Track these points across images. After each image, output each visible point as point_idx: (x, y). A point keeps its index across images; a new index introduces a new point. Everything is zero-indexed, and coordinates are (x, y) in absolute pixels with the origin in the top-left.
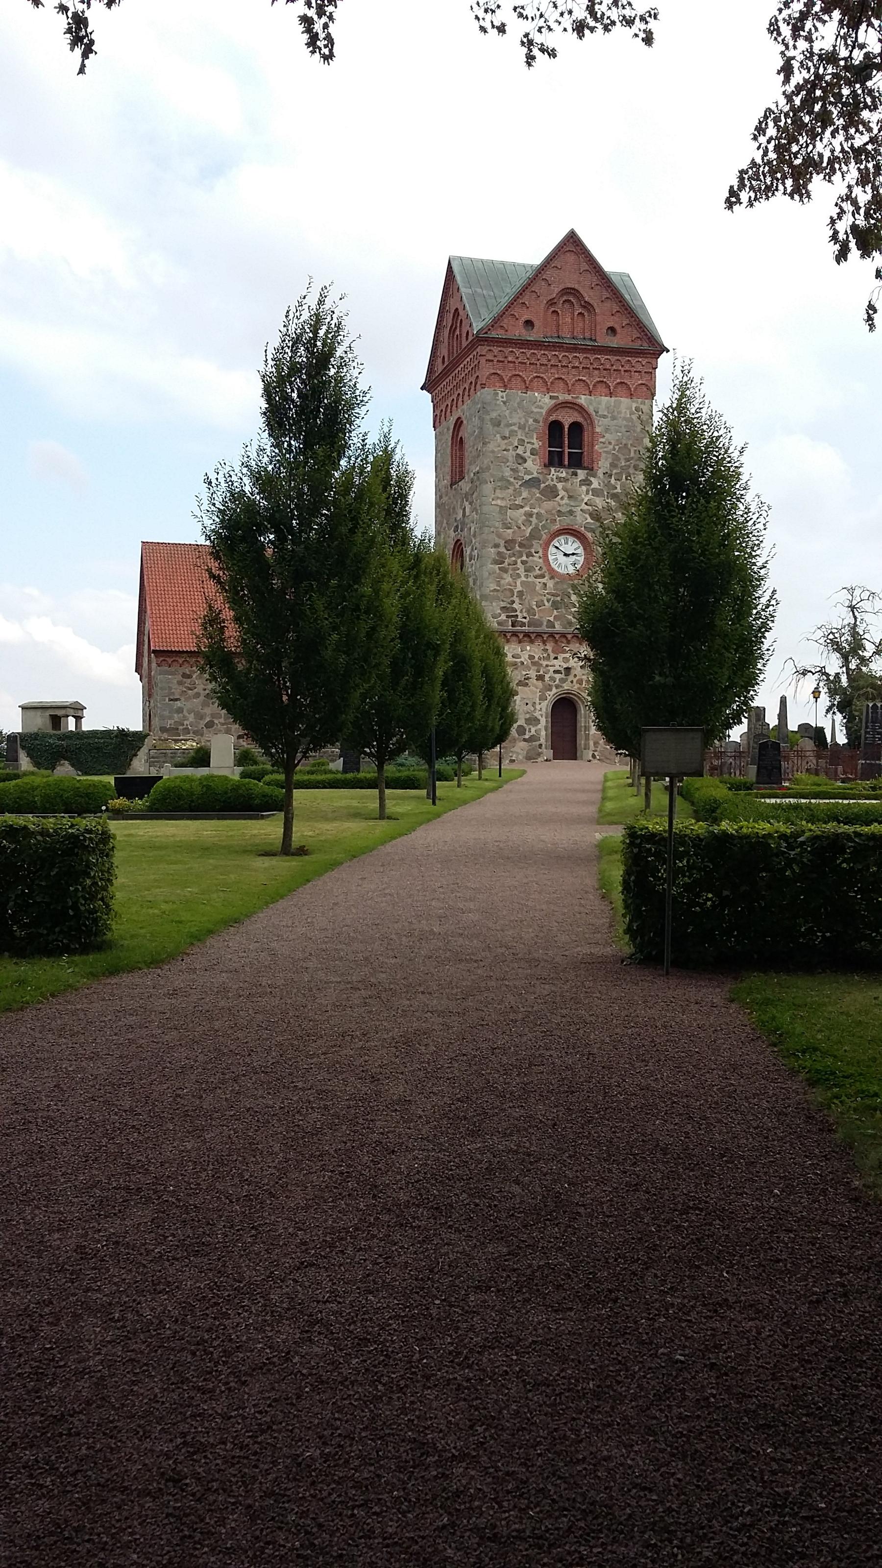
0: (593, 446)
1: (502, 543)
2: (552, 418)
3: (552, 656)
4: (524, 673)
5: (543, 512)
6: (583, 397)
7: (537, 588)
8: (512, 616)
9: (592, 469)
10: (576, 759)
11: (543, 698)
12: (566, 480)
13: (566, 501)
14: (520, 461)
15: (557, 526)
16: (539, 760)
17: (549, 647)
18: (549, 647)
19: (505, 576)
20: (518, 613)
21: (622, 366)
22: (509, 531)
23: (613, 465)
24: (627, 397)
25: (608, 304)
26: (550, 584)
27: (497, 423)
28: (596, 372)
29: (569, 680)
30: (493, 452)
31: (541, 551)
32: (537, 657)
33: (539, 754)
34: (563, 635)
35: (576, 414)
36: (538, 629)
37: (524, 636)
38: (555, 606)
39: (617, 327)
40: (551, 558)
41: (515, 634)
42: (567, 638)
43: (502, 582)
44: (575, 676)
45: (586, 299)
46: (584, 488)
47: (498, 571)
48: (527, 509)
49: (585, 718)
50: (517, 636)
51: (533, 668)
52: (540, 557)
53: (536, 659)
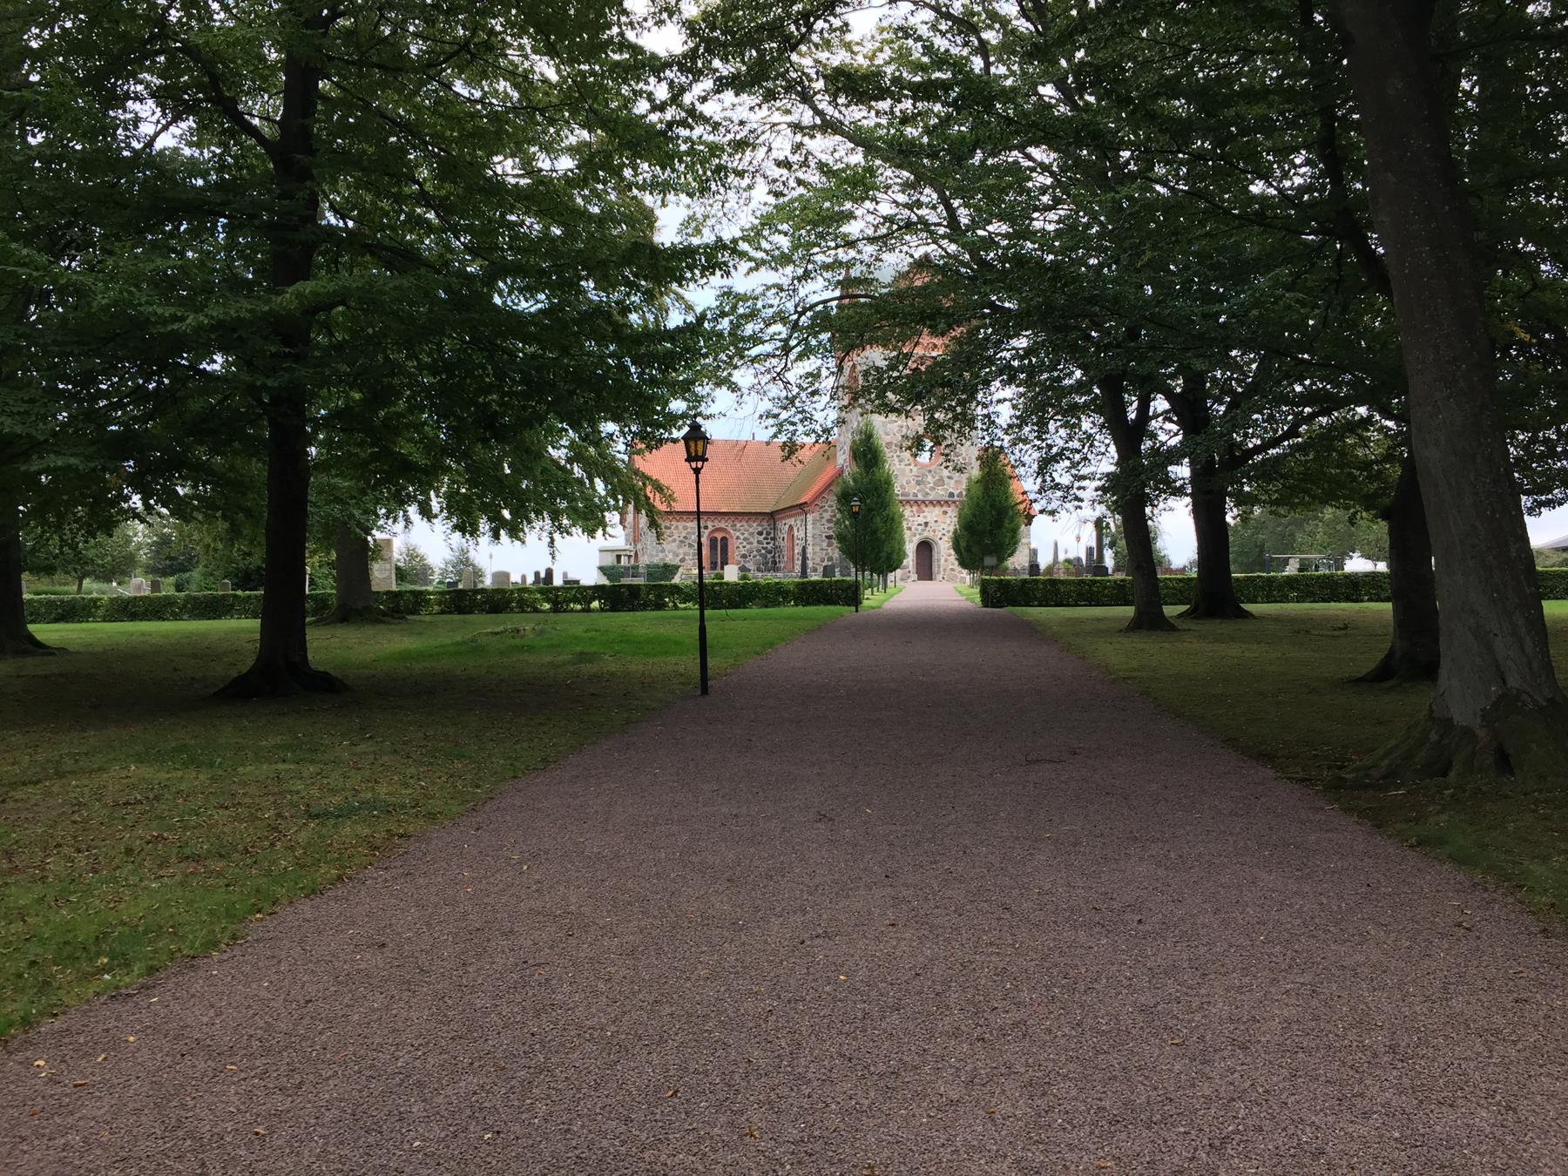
10: (931, 579)
17: (915, 508)
18: (915, 508)
34: (923, 502)
36: (908, 498)
38: (918, 483)
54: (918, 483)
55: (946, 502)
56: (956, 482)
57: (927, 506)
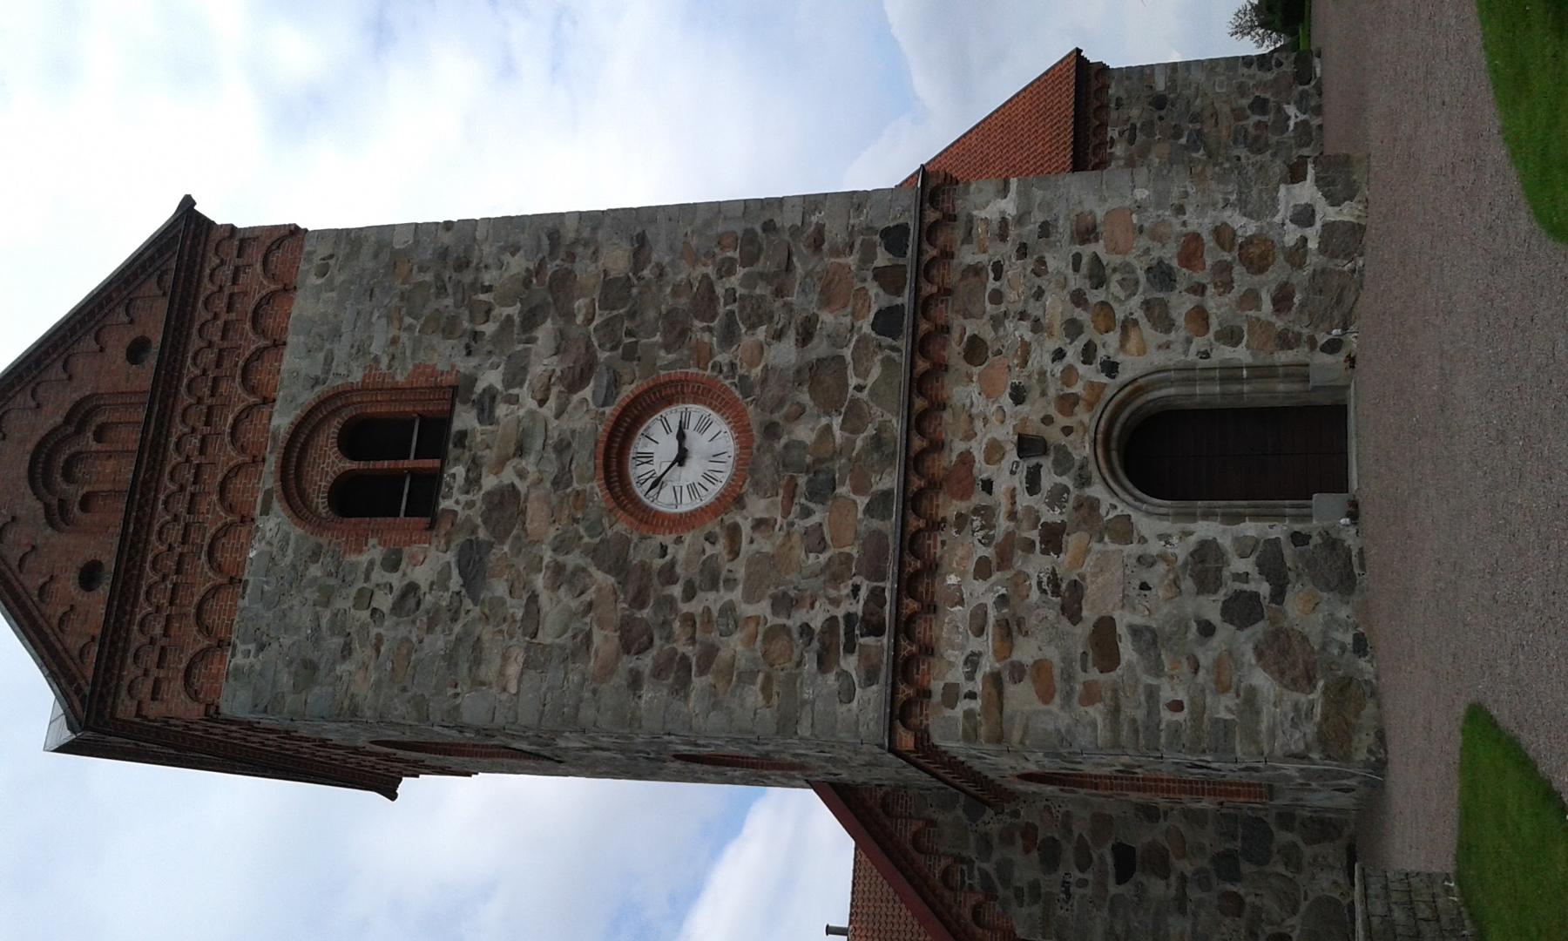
0: (396, 389)
1: (628, 662)
2: (321, 503)
3: (979, 498)
4: (1035, 595)
5: (552, 532)
6: (275, 422)
7: (767, 548)
8: (849, 633)
9: (455, 389)
10: (1337, 414)
11: (1123, 531)
12: (475, 465)
13: (529, 463)
14: (411, 602)
15: (596, 489)
16: (1350, 539)
18: (951, 508)
19: (724, 654)
20: (840, 613)
21: (216, 316)
22: (598, 637)
23: (449, 328)
24: (291, 300)
25: (80, 365)
26: (758, 507)
27: (308, 670)
28: (223, 387)
29: (1063, 440)
30: (378, 685)
31: (660, 538)
32: (982, 551)
33: (1332, 543)
34: (914, 463)
35: (321, 440)
36: (893, 542)
37: (913, 595)
38: (822, 490)
39: (127, 340)
40: (688, 505)
41: (905, 627)
42: (924, 451)
43: (742, 663)
44: (1047, 420)
45: (59, 420)
46: (501, 410)
47: (709, 678)
48: (540, 581)
49: (1190, 381)
50: (912, 618)
51: (1018, 563)
52: (679, 541)
53: (988, 552)
54: (822, 490)
55: (921, 346)
56: (826, 301)
57: (938, 446)
